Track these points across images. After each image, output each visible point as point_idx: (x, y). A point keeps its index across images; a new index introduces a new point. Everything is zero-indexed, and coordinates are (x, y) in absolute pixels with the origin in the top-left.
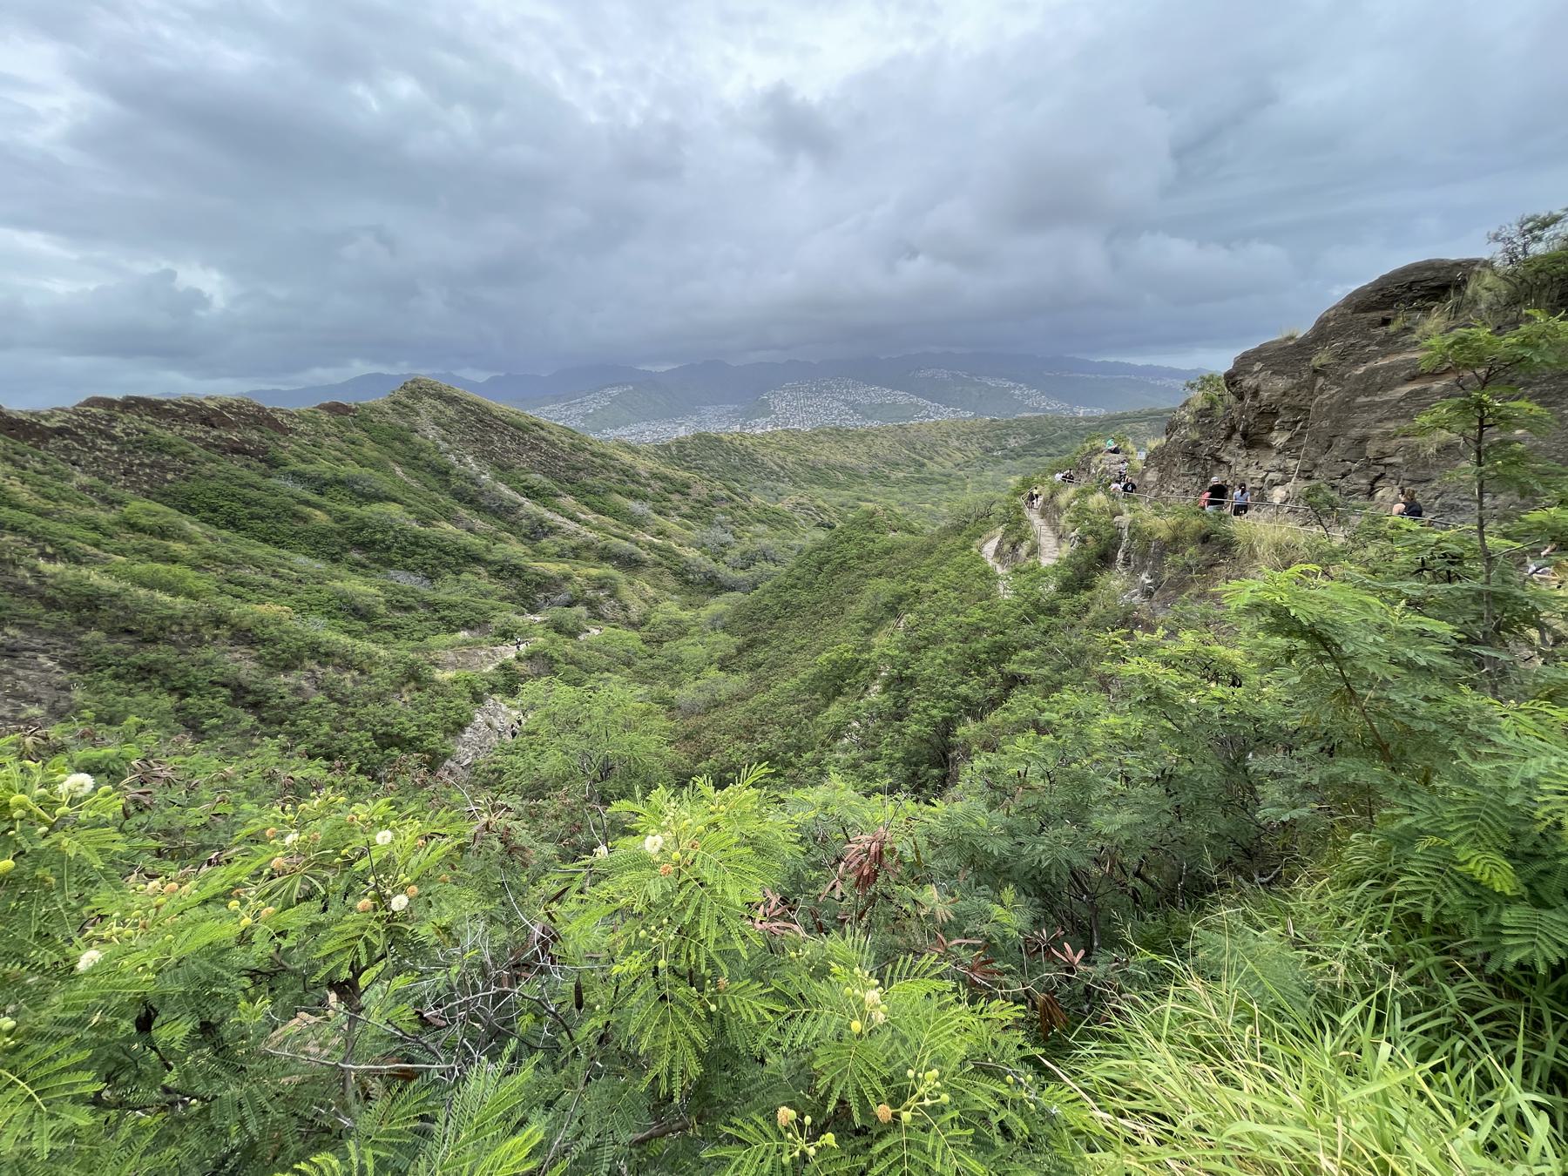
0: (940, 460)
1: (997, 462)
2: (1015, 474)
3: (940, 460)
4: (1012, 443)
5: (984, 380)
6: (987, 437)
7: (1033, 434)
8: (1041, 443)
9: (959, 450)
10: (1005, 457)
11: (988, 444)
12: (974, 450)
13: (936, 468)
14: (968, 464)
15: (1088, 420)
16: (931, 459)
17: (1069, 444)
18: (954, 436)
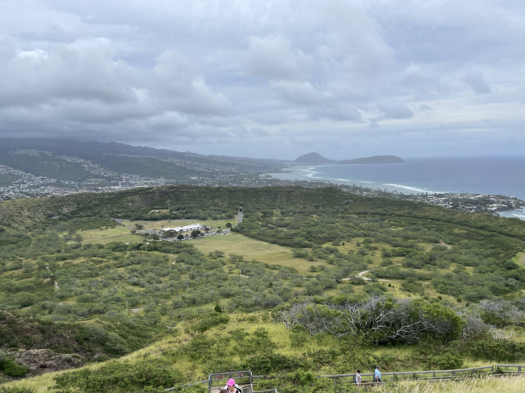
0: (16, 225)
1: (55, 222)
2: (65, 230)
3: (16, 225)
4: (65, 210)
5: (64, 158)
6: (49, 208)
7: (78, 204)
8: (82, 209)
9: (29, 217)
10: (60, 219)
11: (49, 212)
12: (41, 217)
13: (13, 232)
14: (35, 227)
15: (109, 194)
16: (9, 225)
17: (99, 208)
18: (26, 209)
